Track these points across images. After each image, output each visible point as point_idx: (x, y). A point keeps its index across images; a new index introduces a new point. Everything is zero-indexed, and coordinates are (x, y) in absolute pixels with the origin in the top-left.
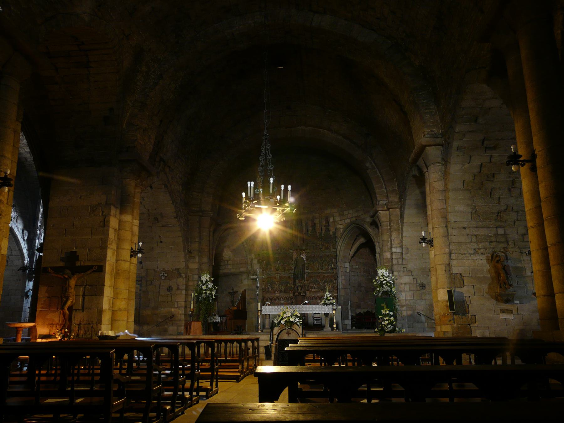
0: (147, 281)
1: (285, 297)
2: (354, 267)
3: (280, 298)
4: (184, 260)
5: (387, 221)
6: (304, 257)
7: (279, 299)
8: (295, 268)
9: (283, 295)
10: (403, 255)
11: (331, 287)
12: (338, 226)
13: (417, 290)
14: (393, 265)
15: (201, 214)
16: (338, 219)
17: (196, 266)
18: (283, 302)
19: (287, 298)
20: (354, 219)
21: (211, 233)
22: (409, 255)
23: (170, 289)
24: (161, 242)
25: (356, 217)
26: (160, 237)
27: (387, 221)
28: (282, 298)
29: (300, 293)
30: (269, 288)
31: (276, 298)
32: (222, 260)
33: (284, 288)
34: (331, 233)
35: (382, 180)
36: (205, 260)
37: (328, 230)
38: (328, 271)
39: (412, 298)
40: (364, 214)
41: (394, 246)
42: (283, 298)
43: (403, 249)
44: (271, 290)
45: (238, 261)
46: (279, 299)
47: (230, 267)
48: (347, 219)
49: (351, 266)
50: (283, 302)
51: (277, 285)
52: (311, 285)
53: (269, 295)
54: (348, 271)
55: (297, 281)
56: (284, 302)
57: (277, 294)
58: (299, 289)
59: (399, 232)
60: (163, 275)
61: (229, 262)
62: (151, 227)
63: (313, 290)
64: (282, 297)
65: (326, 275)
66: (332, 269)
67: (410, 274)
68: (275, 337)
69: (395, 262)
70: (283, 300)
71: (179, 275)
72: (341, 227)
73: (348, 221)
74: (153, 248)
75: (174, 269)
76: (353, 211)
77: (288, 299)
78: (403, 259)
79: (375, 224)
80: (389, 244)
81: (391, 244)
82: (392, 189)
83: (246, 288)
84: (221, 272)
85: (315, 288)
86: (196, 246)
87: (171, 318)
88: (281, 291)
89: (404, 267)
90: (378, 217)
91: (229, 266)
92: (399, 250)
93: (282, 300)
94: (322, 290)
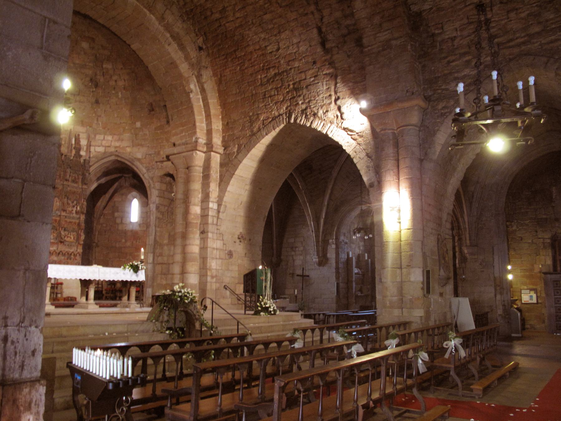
10: (220, 214)
11: (72, 238)
13: (226, 259)
20: (113, 150)
22: (225, 214)
25: (116, 147)
35: (203, 112)
38: (72, 215)
39: (221, 268)
40: (133, 146)
48: (99, 146)
59: (217, 184)
67: (221, 238)
73: (101, 149)
76: (113, 137)
78: (218, 218)
82: (217, 128)
89: (217, 229)
94: (61, 242)
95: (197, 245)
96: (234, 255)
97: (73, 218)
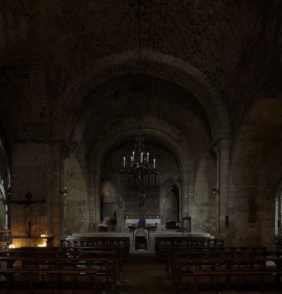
0: (68, 206)
2: (167, 201)
5: (187, 180)
6: (144, 196)
7: (132, 215)
8: (140, 201)
9: (134, 213)
12: (161, 181)
14: (189, 201)
15: (95, 173)
16: (161, 177)
17: (93, 199)
20: (169, 178)
21: (100, 183)
22: (197, 196)
23: (80, 210)
24: (75, 187)
26: (74, 184)
27: (187, 180)
29: (142, 213)
30: (127, 210)
34: (157, 184)
36: (97, 196)
37: (155, 183)
41: (190, 192)
43: (195, 193)
45: (112, 197)
46: (132, 215)
47: (108, 200)
49: (166, 200)
51: (131, 208)
52: (147, 209)
53: (127, 213)
54: (164, 202)
55: (141, 207)
57: (131, 213)
58: (142, 211)
61: (108, 197)
62: (69, 179)
63: (148, 211)
65: (155, 204)
66: (158, 201)
68: (135, 235)
69: (190, 199)
72: (162, 181)
73: (166, 179)
77: (136, 216)
78: (194, 198)
79: (180, 181)
80: (187, 191)
81: (189, 191)
84: (104, 202)
85: (149, 211)
86: (93, 189)
88: (133, 212)
90: (182, 177)
92: (192, 194)
95: (187, 209)
96: (204, 212)
97: (156, 203)
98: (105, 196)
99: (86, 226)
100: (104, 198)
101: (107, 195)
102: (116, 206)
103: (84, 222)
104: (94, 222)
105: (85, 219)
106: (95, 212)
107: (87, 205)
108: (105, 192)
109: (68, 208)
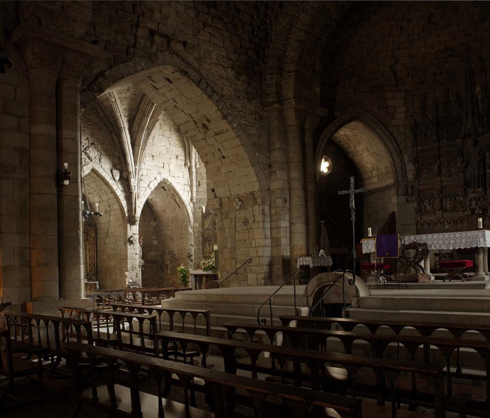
0: (222, 214)
1: (452, 219)
3: (444, 222)
4: (256, 179)
18: (447, 227)
19: (454, 221)
23: (246, 222)
28: (445, 221)
30: (426, 207)
31: (436, 222)
32: (365, 172)
33: (450, 204)
36: (295, 174)
42: (447, 221)
44: (429, 208)
45: (384, 170)
47: (375, 180)
50: (447, 227)
56: (450, 227)
60: (237, 204)
61: (374, 173)
64: (445, 219)
70: (449, 223)
71: (255, 199)
74: (218, 167)
75: (249, 193)
83: (395, 209)
87: (249, 263)
91: (373, 178)
93: (446, 224)
98: (367, 170)
99: (259, 265)
100: (366, 176)
101: (369, 165)
102: (395, 197)
103: (255, 255)
104: (287, 253)
105: (257, 245)
106: (291, 224)
107: (260, 203)
108: (364, 158)
109: (222, 220)
